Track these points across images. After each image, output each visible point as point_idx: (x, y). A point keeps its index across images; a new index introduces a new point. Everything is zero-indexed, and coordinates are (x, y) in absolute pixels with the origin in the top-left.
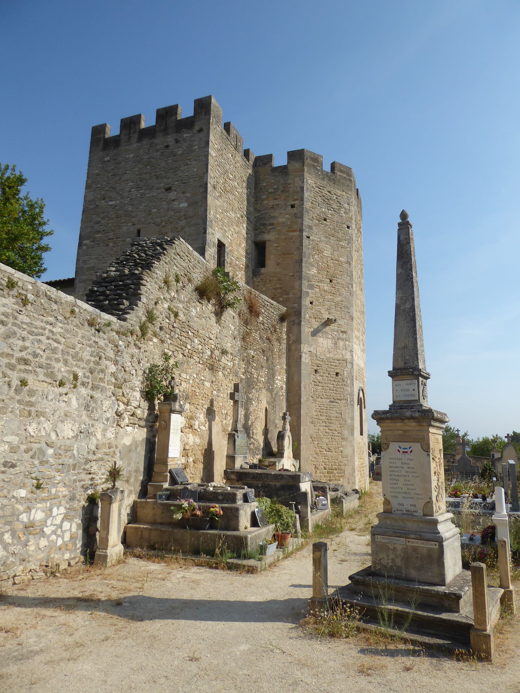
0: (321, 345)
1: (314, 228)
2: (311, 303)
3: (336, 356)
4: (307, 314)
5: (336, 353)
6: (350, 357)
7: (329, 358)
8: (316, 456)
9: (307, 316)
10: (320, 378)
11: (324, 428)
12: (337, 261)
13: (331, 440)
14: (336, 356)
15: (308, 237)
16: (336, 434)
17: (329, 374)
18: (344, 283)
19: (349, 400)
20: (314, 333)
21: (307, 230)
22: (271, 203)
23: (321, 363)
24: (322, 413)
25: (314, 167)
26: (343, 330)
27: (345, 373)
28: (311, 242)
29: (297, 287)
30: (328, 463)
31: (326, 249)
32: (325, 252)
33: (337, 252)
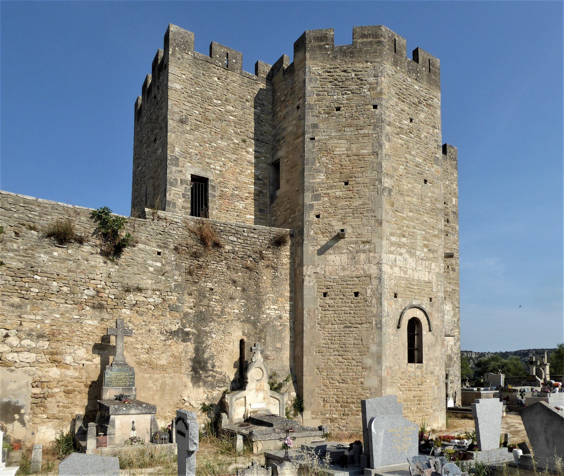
0: (332, 263)
1: (321, 125)
2: (318, 216)
3: (355, 273)
4: (310, 232)
5: (353, 269)
6: (376, 271)
7: (344, 276)
8: (324, 388)
9: (312, 233)
10: (328, 302)
11: (336, 357)
12: (356, 155)
13: (346, 370)
14: (355, 273)
15: (313, 139)
16: (354, 363)
17: (344, 296)
18: (367, 180)
19: (374, 323)
20: (322, 251)
21: (311, 130)
23: (332, 284)
24: (332, 341)
25: (320, 47)
26: (365, 239)
27: (369, 291)
28: (316, 144)
29: (301, 202)
30: (341, 396)
31: (338, 145)
32: (337, 149)
33: (357, 145)
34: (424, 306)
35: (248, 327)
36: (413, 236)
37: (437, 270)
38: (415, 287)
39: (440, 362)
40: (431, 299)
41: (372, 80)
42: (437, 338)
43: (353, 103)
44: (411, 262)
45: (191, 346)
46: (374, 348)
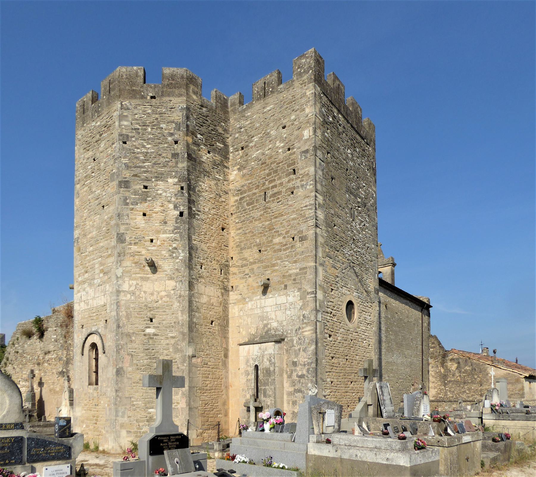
34: (100, 331)
36: (93, 268)
37: (111, 290)
38: (94, 314)
39: (112, 384)
40: (106, 321)
42: (109, 360)
44: (91, 292)
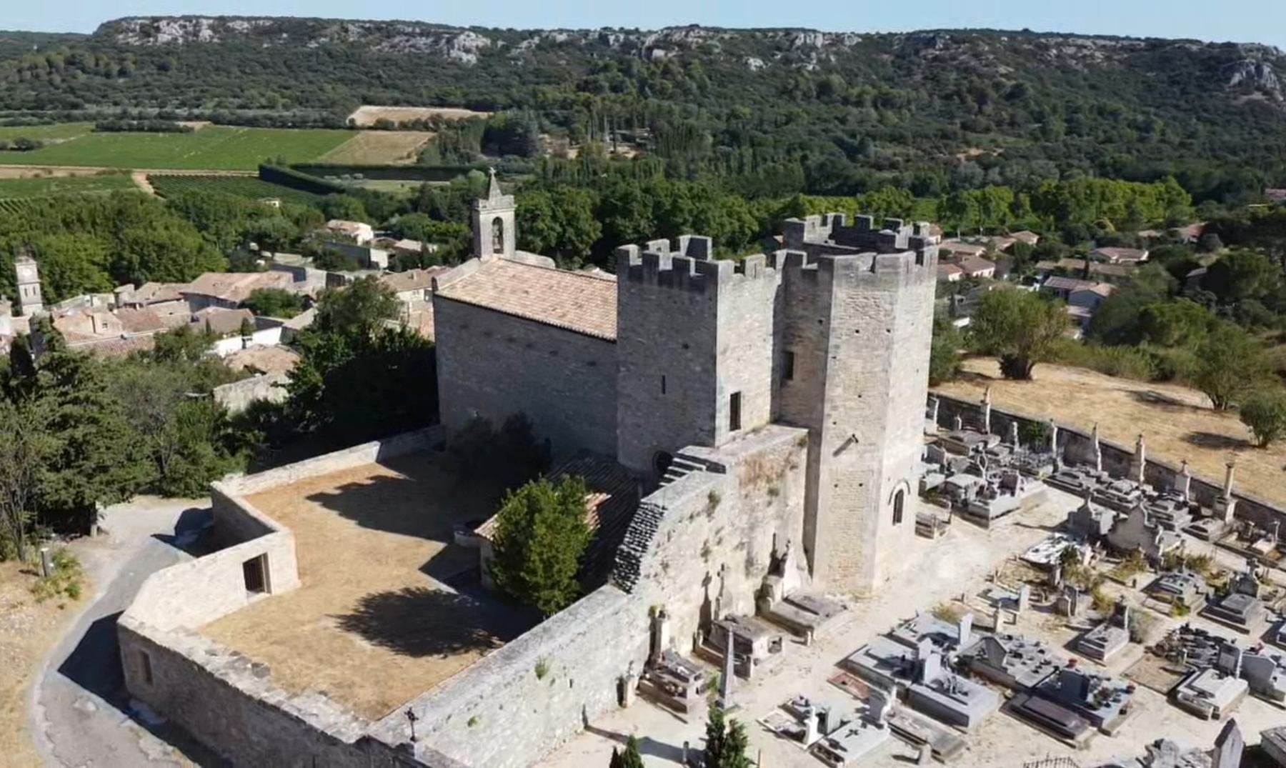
20: (836, 453)
22: (801, 312)
35: (778, 522)
41: (888, 307)
43: (870, 327)
45: (745, 552)
46: (871, 526)
